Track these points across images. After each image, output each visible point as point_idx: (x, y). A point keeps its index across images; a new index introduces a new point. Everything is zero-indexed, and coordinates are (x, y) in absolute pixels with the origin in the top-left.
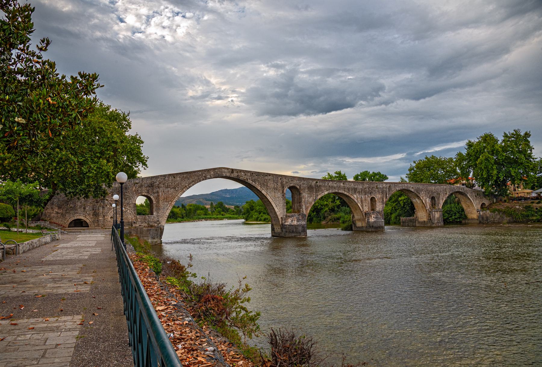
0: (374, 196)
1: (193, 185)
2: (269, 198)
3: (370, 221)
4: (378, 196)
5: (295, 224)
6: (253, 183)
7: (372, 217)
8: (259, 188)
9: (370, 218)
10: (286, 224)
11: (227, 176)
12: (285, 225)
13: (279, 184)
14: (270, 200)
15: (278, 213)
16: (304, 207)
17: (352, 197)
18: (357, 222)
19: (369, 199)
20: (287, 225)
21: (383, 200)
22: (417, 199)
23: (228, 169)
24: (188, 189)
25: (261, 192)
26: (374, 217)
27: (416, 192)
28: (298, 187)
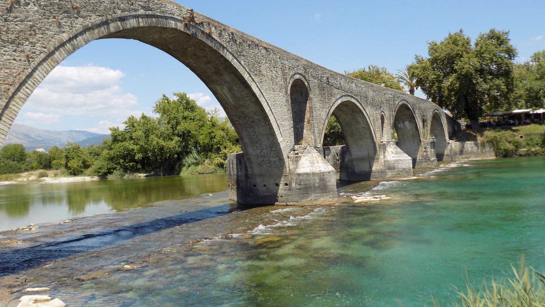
0: (383, 113)
1: (87, 42)
2: (264, 104)
3: (389, 159)
4: (387, 113)
5: (323, 170)
6: (235, 61)
7: (390, 153)
8: (246, 76)
9: (386, 154)
10: (301, 170)
11: (179, 28)
12: (299, 175)
13: (280, 72)
14: (267, 110)
15: (282, 146)
16: (316, 131)
17: (364, 112)
18: (355, 163)
19: (379, 117)
20: (304, 174)
21: (391, 121)
22: (407, 123)
23: (180, 7)
24: (69, 53)
25: (248, 87)
26: (392, 152)
27: (412, 110)
28: (306, 84)
